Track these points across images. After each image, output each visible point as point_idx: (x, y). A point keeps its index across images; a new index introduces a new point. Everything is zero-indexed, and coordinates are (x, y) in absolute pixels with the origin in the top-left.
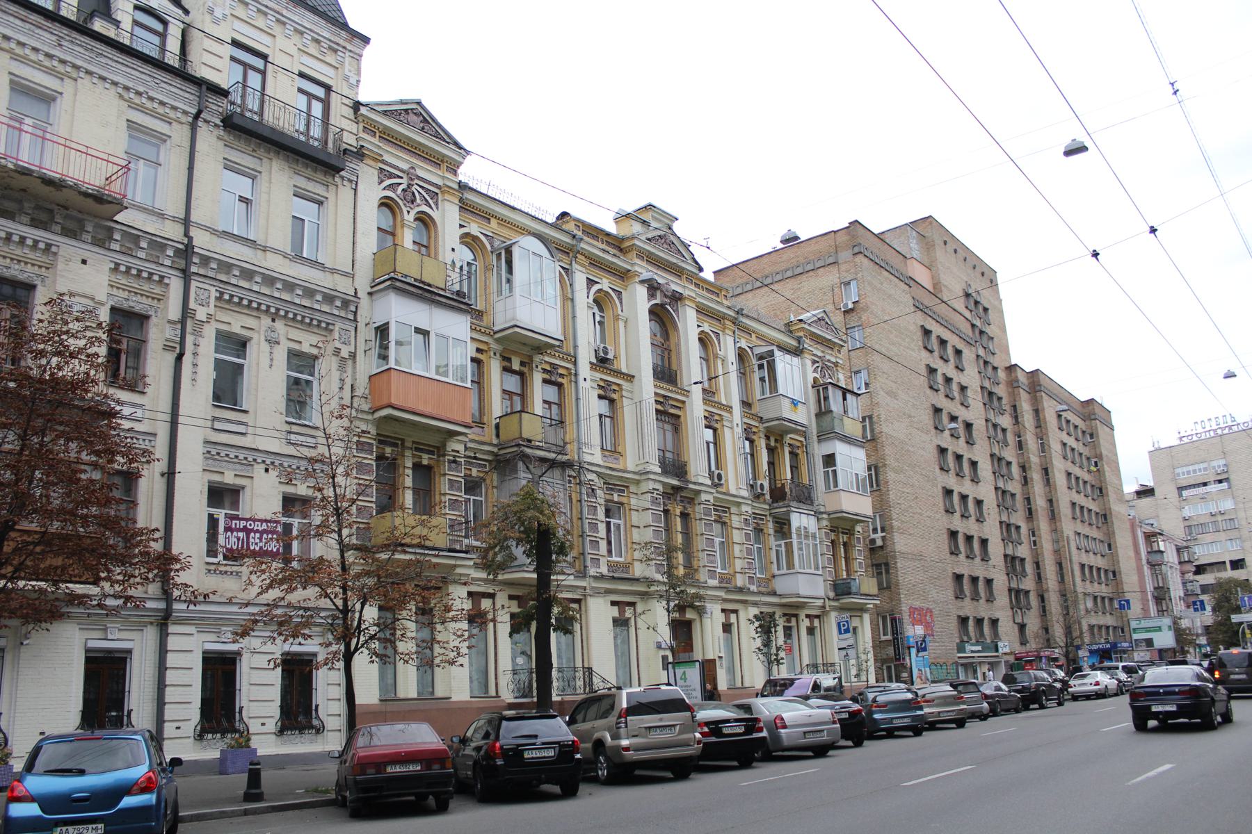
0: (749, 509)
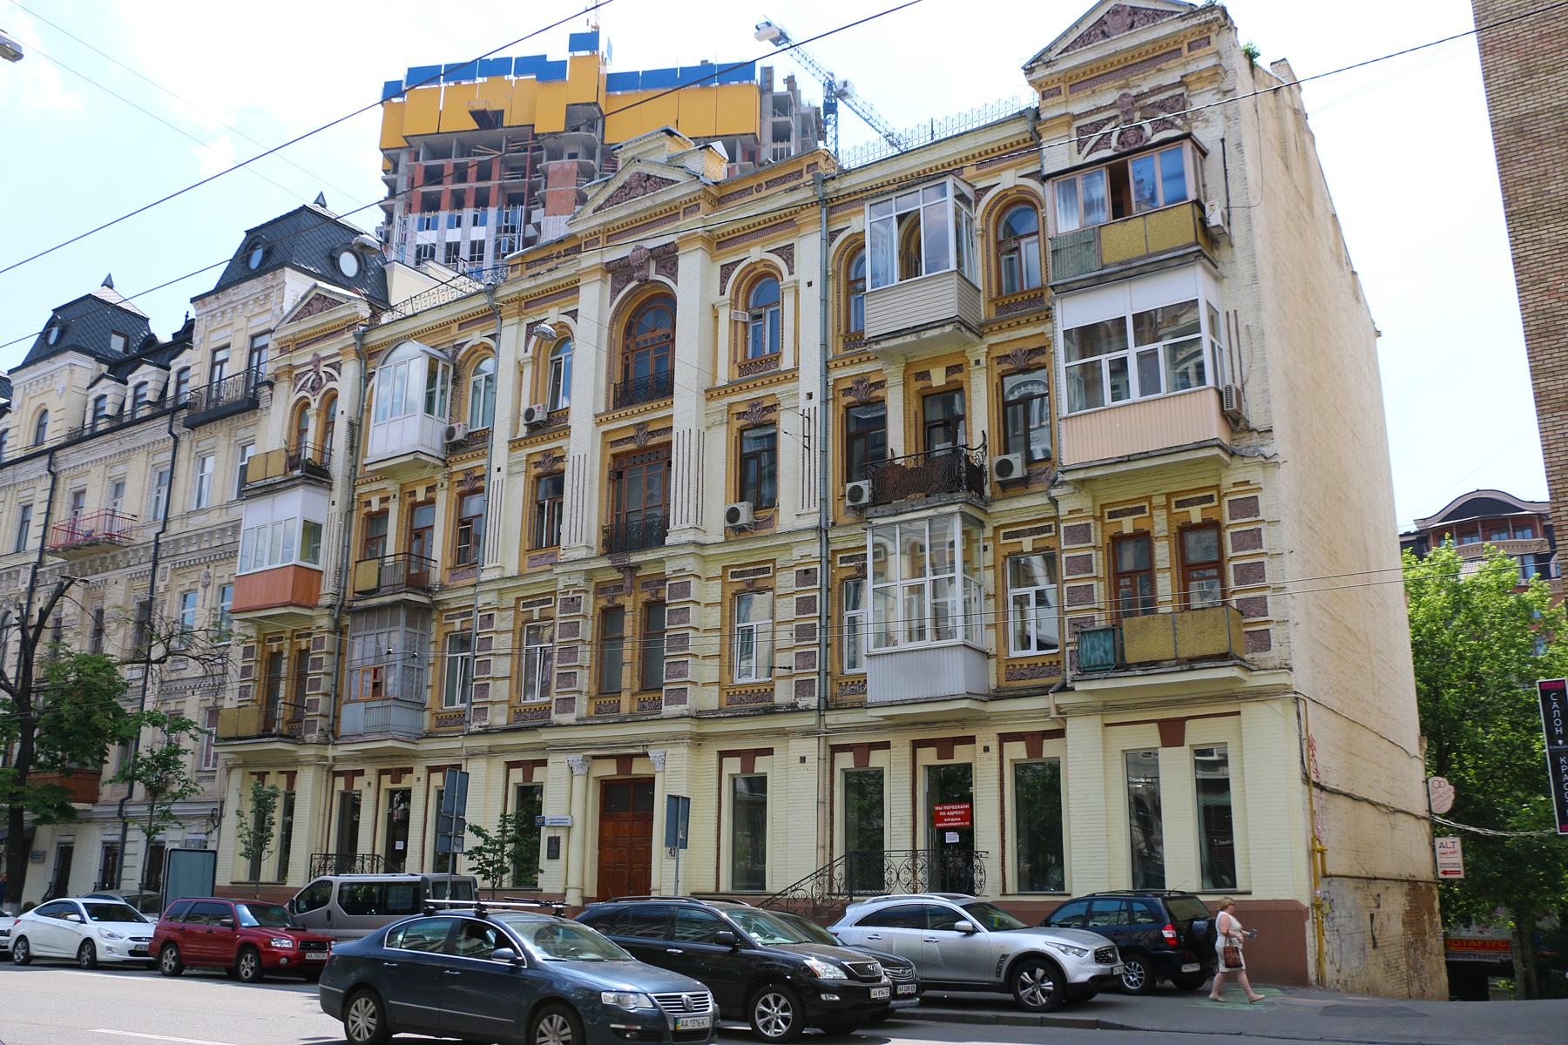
0: (815, 550)
